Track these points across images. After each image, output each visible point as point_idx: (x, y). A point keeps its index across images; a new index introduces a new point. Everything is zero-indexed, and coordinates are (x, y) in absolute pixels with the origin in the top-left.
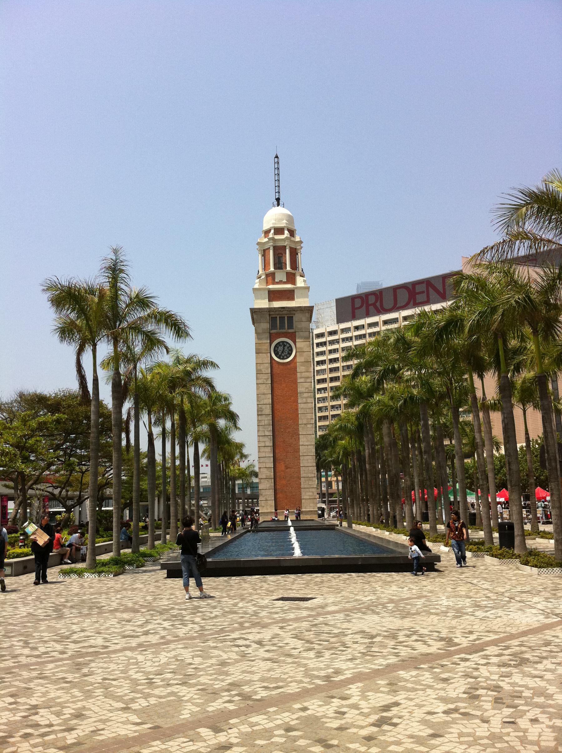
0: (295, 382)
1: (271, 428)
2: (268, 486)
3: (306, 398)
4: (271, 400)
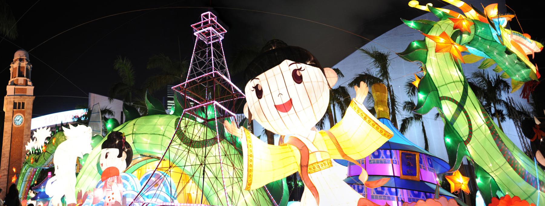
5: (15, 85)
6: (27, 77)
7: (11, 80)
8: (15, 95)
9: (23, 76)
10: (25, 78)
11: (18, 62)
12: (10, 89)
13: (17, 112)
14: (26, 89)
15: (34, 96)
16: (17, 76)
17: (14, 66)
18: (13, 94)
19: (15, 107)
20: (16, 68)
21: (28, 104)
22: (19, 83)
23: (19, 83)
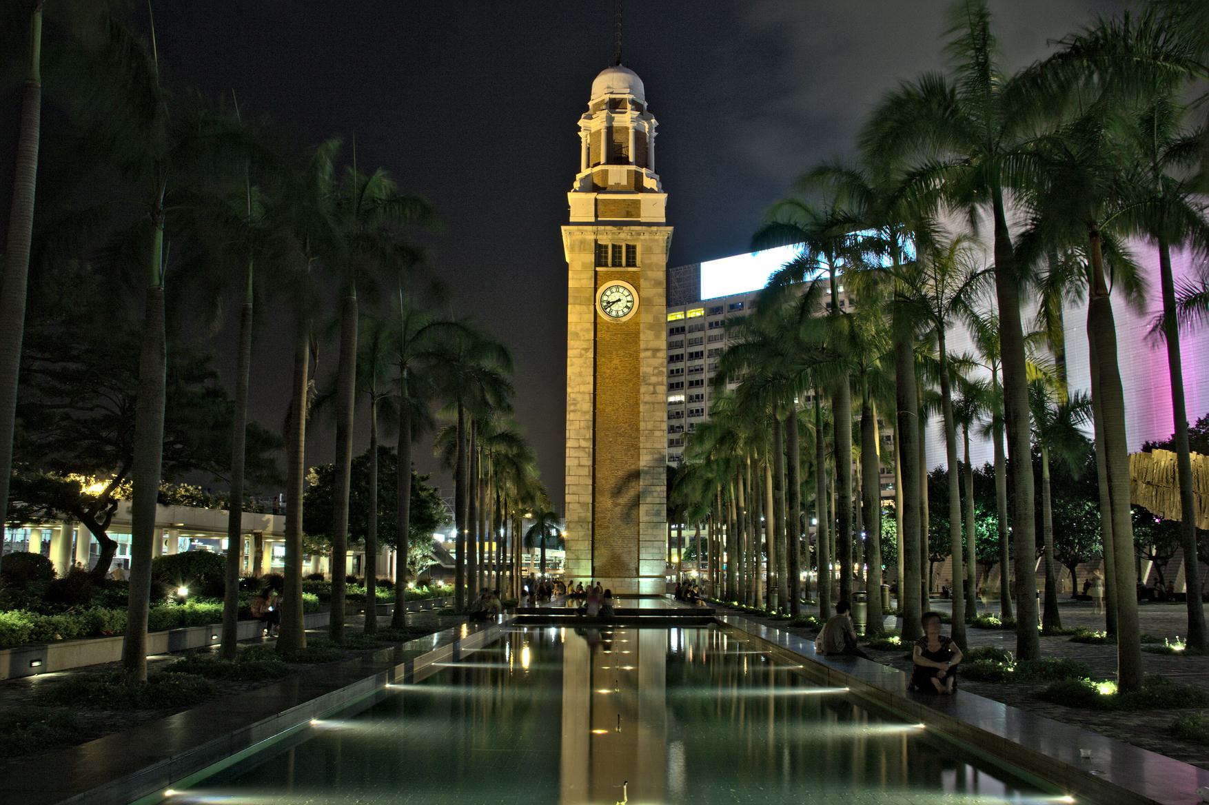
0: (637, 358)
1: (589, 434)
2: (581, 534)
3: (654, 385)
4: (591, 387)
5: (596, 189)
6: (642, 161)
7: (585, 172)
8: (597, 223)
9: (625, 161)
10: (633, 168)
11: (602, 115)
12: (580, 203)
13: (610, 277)
14: (637, 202)
15: (667, 224)
16: (603, 160)
17: (591, 127)
18: (593, 220)
19: (600, 260)
20: (599, 132)
21: (648, 250)
22: (611, 182)
23: (611, 182)
